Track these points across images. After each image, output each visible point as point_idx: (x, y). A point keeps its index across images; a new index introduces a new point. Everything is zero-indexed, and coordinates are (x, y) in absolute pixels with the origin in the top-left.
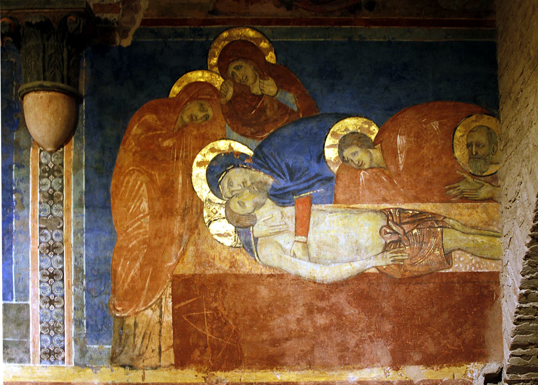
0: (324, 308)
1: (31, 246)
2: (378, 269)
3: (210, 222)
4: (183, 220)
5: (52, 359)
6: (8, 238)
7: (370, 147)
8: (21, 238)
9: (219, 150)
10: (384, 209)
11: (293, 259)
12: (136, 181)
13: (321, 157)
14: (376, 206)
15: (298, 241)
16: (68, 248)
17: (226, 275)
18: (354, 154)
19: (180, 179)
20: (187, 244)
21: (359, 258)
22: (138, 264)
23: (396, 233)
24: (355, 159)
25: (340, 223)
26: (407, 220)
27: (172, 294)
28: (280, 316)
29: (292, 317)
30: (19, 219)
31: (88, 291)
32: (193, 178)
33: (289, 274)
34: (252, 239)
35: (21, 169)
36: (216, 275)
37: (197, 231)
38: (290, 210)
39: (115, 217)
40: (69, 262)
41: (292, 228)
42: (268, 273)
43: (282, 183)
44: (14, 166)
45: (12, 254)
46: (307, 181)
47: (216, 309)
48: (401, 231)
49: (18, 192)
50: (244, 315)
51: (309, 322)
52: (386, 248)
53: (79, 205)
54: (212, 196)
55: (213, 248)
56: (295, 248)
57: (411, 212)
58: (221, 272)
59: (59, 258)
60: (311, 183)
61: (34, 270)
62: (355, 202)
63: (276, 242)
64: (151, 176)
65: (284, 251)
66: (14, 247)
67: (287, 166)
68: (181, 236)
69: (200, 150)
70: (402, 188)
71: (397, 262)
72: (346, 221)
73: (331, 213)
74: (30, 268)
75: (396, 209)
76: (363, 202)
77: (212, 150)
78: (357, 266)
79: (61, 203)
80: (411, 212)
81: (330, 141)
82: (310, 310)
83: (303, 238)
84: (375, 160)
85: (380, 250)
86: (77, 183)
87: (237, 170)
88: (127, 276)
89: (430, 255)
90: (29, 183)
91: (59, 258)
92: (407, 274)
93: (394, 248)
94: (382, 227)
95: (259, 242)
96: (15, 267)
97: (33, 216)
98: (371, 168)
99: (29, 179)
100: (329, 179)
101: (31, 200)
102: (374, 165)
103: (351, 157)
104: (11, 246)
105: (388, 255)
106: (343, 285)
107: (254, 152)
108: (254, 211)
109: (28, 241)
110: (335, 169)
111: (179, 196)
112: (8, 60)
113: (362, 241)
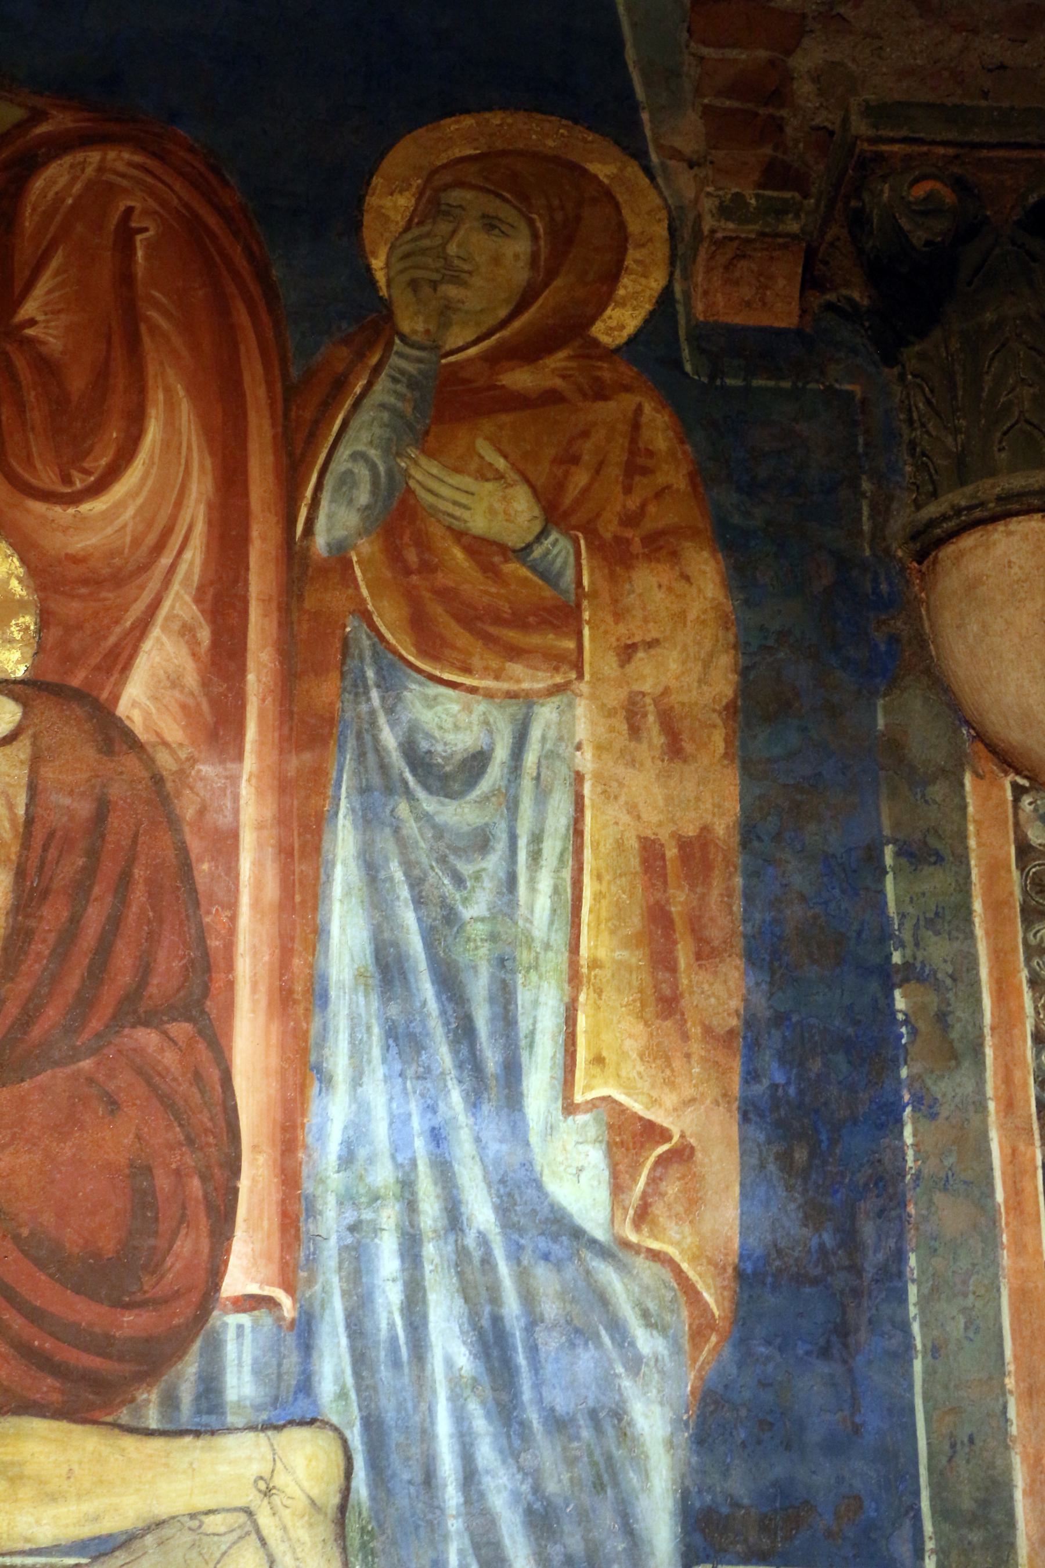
1: (1006, 1259)
6: (881, 1213)
30: (934, 1116)
35: (927, 870)
44: (889, 851)
45: (902, 1298)
49: (921, 979)
66: (913, 1260)
74: (1010, 1383)
90: (971, 936)
96: (929, 1373)
97: (1009, 1106)
99: (968, 920)
101: (988, 1019)
104: (900, 1256)
112: (830, 387)
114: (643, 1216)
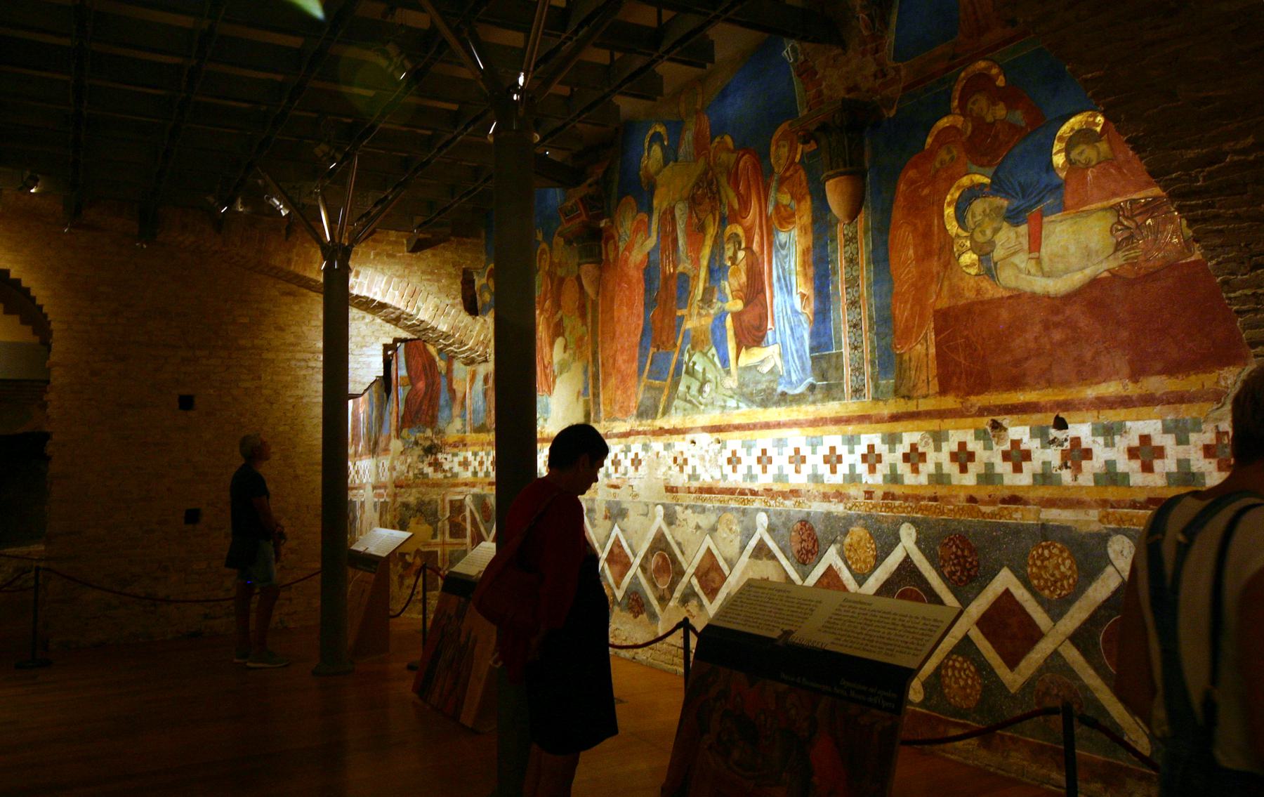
0: (1059, 323)
2: (1110, 272)
3: (960, 256)
4: (939, 259)
5: (858, 396)
7: (1097, 141)
8: (835, 297)
9: (963, 186)
10: (1115, 205)
11: (1029, 278)
12: (905, 232)
13: (1049, 166)
14: (1105, 204)
15: (1032, 258)
16: (863, 301)
17: (973, 304)
18: (1081, 153)
19: (936, 221)
20: (943, 280)
21: (1090, 264)
22: (909, 306)
23: (1127, 228)
24: (1082, 158)
25: (1070, 230)
26: (1138, 212)
27: (934, 328)
28: (1019, 336)
29: (1030, 336)
31: (877, 334)
32: (946, 217)
33: (1025, 293)
34: (992, 265)
36: (965, 306)
37: (949, 267)
38: (1024, 229)
39: (892, 267)
40: (864, 312)
41: (1026, 247)
42: (1008, 295)
43: (1016, 203)
46: (1039, 194)
47: (967, 338)
48: (1132, 225)
50: (990, 339)
51: (1046, 339)
52: (1118, 246)
53: (868, 263)
54: (960, 231)
55: (962, 279)
56: (1029, 266)
57: (1143, 201)
58: (969, 301)
59: (858, 310)
60: (1041, 195)
61: (844, 323)
62: (1085, 204)
63: (1012, 263)
64: (915, 225)
65: (1020, 271)
67: (1020, 184)
68: (938, 273)
69: (949, 190)
70: (1133, 176)
71: (1129, 261)
72: (1075, 227)
73: (1061, 221)
75: (1127, 201)
76: (1092, 203)
77: (958, 188)
78: (1089, 272)
79: (858, 263)
80: (1143, 201)
81: (1057, 146)
82: (1047, 326)
83: (1035, 255)
84: (1102, 154)
85: (1111, 250)
86: (867, 245)
87: (979, 200)
88: (902, 317)
89: (1167, 244)
91: (858, 310)
92: (1142, 271)
93: (1126, 246)
94: (1113, 225)
95: (998, 266)
98: (1099, 163)
100: (1059, 187)
102: (1102, 159)
103: (1078, 158)
105: (1120, 254)
106: (1076, 295)
107: (992, 179)
108: (993, 237)
109: (839, 300)
110: (1063, 175)
111: (936, 238)
113: (1092, 245)
114: (804, 308)
